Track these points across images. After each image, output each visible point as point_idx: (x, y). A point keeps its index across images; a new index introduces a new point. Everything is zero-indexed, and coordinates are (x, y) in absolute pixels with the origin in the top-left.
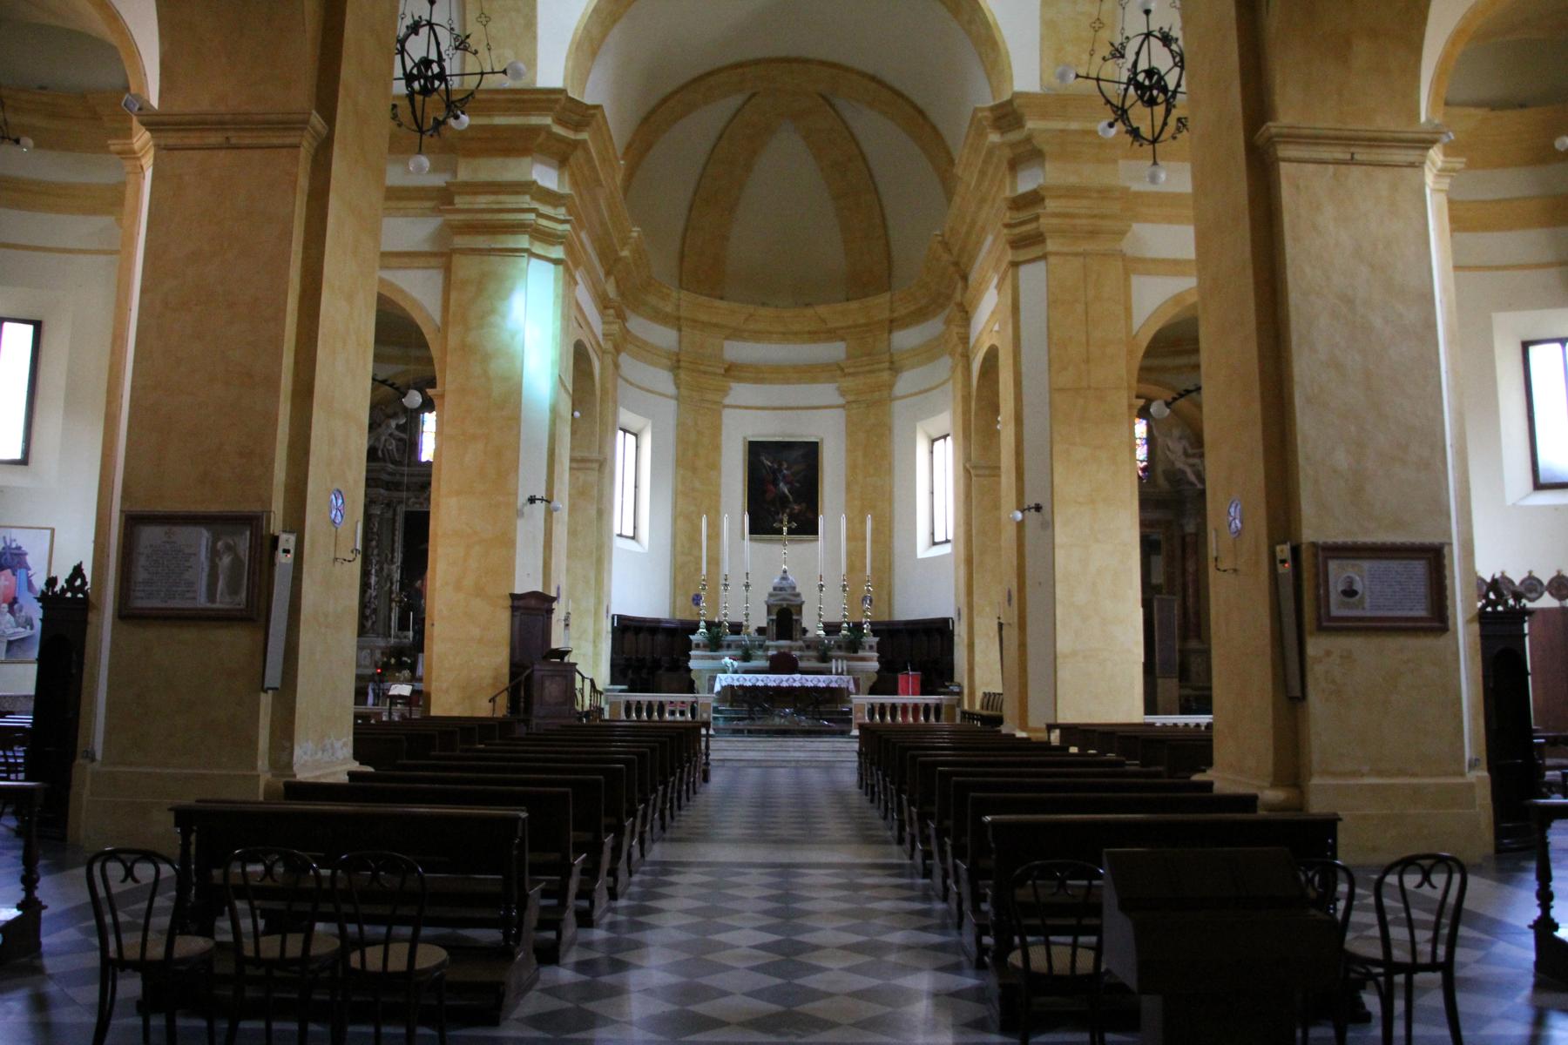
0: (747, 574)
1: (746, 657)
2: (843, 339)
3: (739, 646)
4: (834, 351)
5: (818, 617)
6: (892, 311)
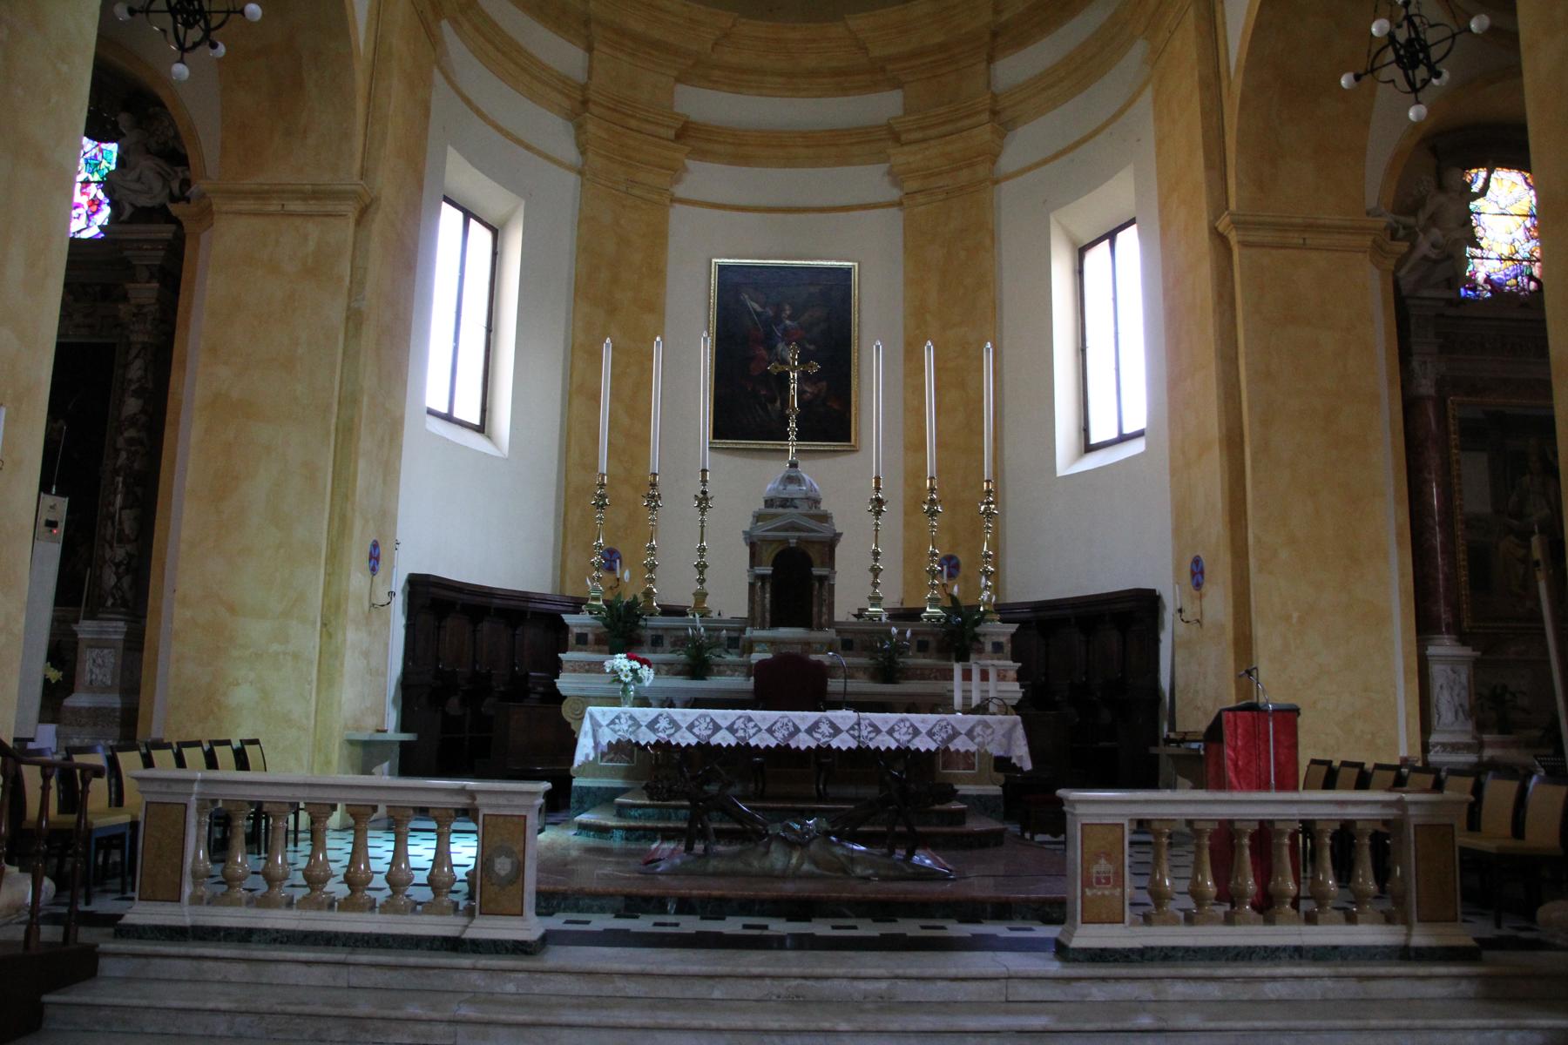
0: (704, 471)
1: (698, 668)
2: (897, 84)
3: (679, 643)
4: (884, 105)
5: (871, 575)
6: (997, 11)
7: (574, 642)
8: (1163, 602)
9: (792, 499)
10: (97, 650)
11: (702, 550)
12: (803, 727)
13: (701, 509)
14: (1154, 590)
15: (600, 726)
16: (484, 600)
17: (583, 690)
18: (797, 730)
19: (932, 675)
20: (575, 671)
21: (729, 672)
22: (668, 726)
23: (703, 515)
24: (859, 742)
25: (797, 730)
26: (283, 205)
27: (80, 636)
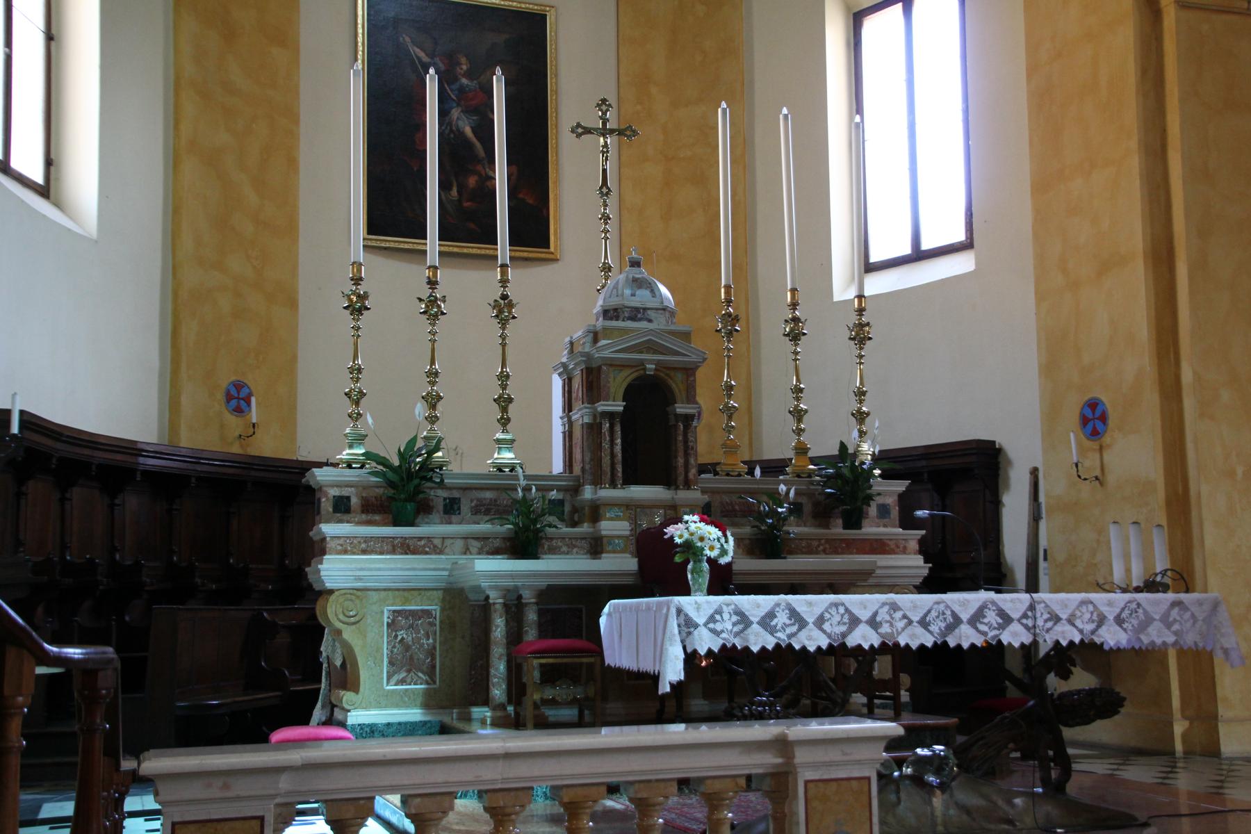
7: (331, 510)
8: (1006, 455)
9: (645, 309)
11: (504, 378)
12: (965, 616)
13: (501, 320)
14: (994, 442)
15: (696, 626)
16: (87, 452)
17: (359, 579)
18: (957, 621)
19: (821, 548)
20: (345, 552)
21: (565, 549)
22: (788, 622)
23: (503, 328)
24: (1035, 635)
25: (957, 621)
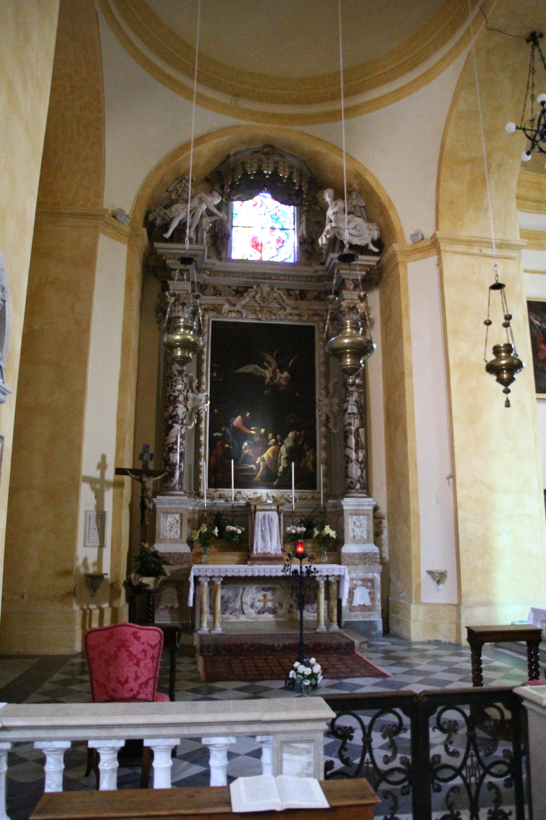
10: (355, 517)
26: (480, 250)
27: (345, 508)
